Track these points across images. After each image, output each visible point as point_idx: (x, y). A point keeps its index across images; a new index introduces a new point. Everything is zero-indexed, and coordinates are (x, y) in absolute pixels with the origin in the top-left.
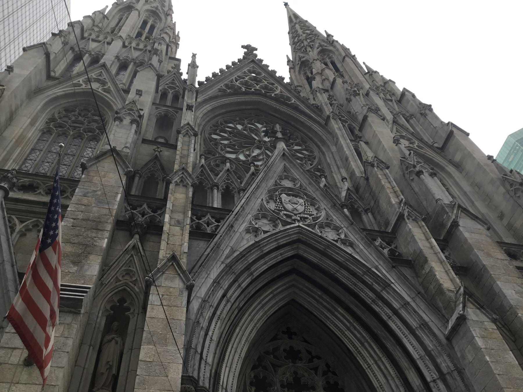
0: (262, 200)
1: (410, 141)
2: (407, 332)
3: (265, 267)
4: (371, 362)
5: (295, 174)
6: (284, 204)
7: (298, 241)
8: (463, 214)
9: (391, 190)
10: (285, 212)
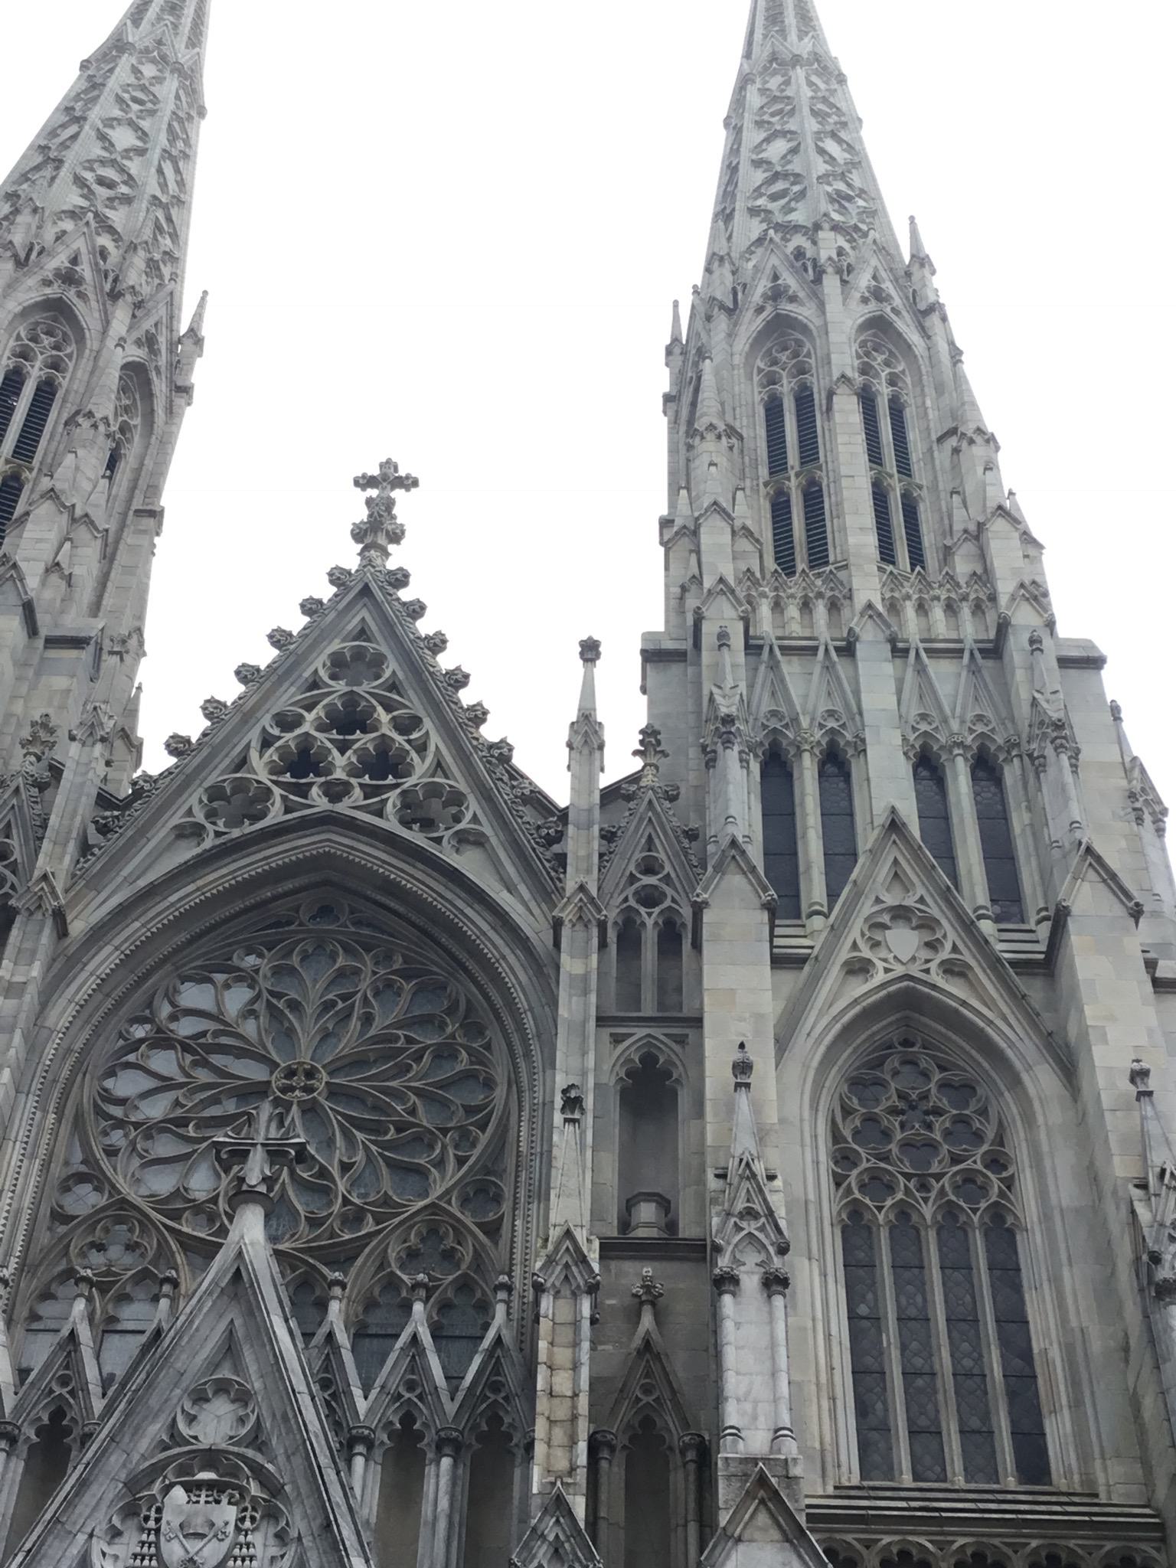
0: (91, 1536)
1: (933, 930)
5: (253, 1369)
6: (162, 1539)
8: (763, 1518)
9: (562, 1412)
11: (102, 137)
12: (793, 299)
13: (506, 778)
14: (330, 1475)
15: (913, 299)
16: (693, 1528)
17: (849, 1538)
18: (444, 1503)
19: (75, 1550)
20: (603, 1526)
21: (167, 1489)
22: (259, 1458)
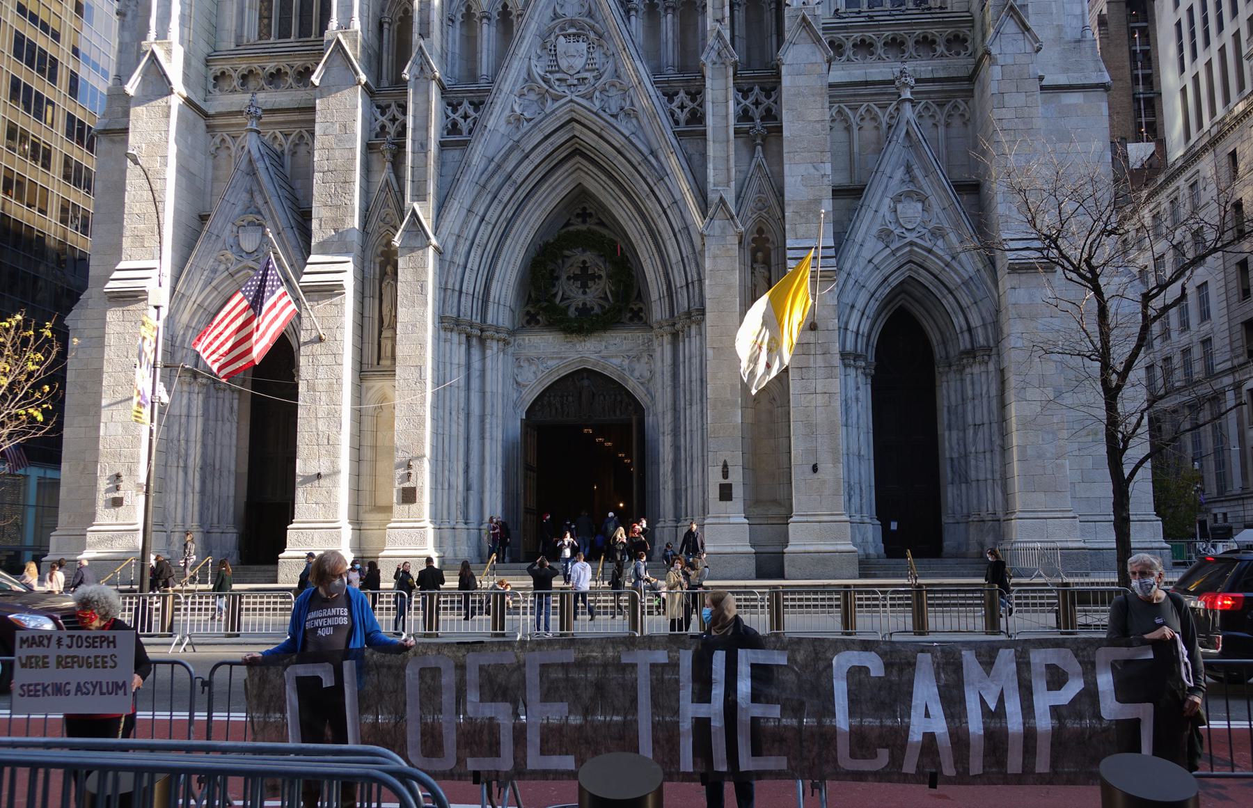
2: (672, 235)
3: (532, 167)
4: (647, 256)
7: (572, 120)
8: (804, 34)
10: (558, 76)
14: (623, 26)
16: (774, 37)
17: (840, 36)
18: (670, 34)
19: (525, 66)
20: (737, 39)
21: (557, 38)
22: (593, 23)
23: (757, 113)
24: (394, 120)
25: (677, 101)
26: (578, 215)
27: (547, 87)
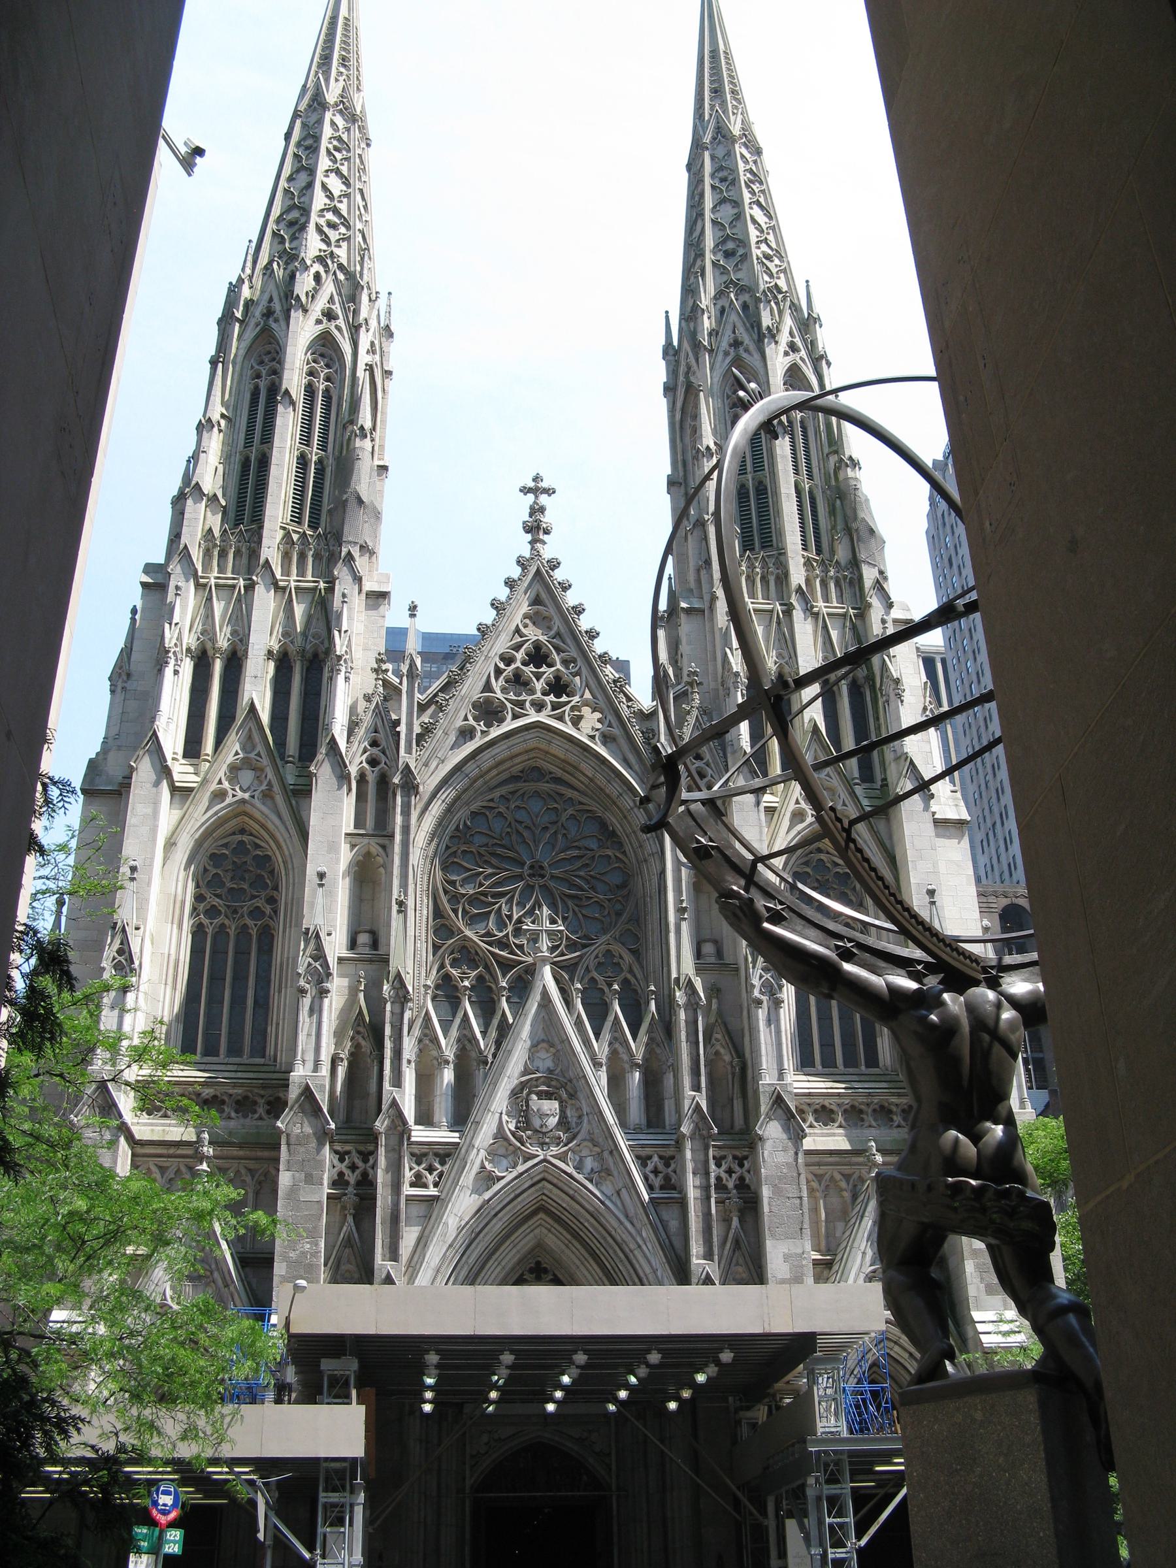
7: (544, 1179)
11: (324, 187)
12: (747, 350)
13: (624, 700)
15: (811, 346)
21: (528, 1094)
23: (731, 1185)
24: (353, 1167)
25: (650, 1166)
26: (531, 1271)
27: (519, 1145)
